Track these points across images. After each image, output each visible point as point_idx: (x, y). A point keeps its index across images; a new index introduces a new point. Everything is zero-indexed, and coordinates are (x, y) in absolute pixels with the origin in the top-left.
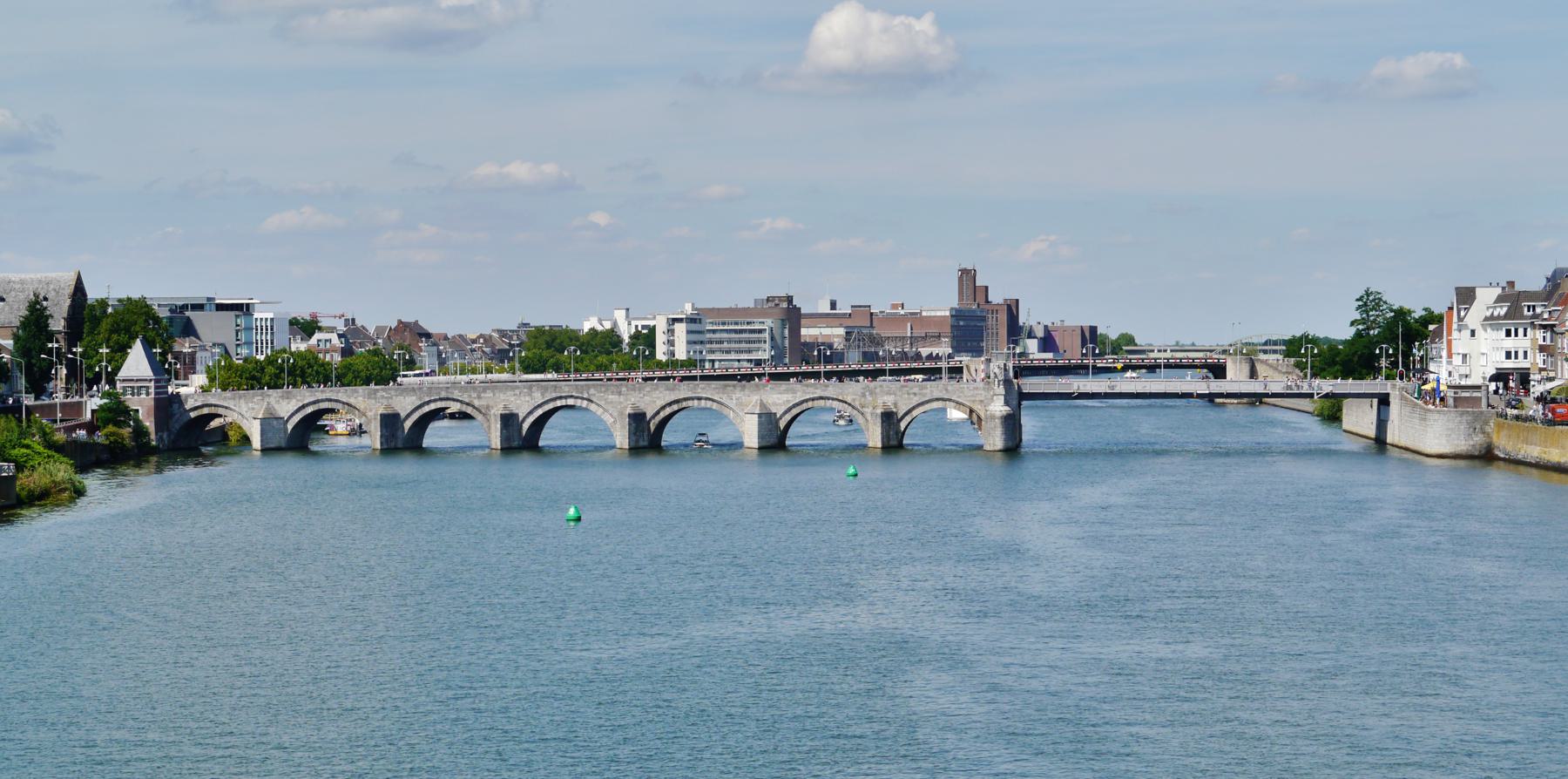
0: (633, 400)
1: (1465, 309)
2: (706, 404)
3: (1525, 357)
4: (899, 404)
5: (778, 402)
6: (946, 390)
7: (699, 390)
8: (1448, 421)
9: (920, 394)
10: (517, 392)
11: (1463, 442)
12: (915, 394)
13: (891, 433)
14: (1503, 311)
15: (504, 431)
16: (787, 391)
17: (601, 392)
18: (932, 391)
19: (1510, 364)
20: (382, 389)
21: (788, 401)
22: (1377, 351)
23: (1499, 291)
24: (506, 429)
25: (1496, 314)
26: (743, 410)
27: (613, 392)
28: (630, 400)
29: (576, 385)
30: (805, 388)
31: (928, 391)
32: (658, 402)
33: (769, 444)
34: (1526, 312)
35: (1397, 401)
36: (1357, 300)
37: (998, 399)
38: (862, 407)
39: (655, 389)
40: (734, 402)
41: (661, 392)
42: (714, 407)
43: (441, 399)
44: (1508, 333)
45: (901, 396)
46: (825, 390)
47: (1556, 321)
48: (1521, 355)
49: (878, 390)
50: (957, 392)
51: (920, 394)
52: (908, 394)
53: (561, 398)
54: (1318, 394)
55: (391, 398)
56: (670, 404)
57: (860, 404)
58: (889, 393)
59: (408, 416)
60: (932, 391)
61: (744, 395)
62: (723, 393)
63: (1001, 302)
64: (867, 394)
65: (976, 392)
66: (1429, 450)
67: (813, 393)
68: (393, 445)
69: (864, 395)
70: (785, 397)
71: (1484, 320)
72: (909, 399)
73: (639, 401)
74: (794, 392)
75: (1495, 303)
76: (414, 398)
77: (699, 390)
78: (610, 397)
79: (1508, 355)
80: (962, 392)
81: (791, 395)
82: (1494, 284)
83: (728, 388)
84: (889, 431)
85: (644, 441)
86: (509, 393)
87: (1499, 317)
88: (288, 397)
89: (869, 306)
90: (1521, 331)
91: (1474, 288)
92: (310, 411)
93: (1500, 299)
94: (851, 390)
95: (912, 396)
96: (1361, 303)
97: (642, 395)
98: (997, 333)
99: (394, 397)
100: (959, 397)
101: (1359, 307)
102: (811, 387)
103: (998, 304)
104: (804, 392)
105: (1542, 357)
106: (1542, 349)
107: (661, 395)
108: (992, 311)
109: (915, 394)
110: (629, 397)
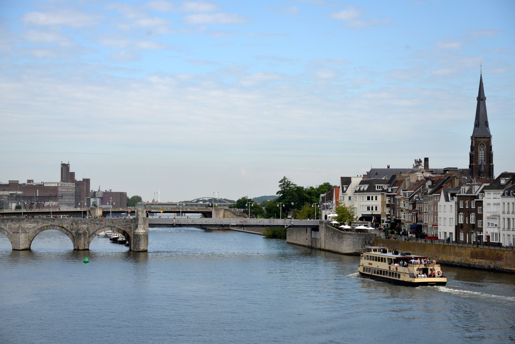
1: (346, 187)
3: (376, 210)
4: (90, 229)
5: (30, 227)
6: (113, 222)
8: (354, 238)
9: (100, 224)
11: (361, 248)
12: (97, 224)
13: (86, 243)
14: (366, 188)
16: (34, 222)
18: (105, 223)
19: (369, 213)
21: (35, 227)
22: (278, 206)
23: (361, 179)
25: (362, 189)
26: (12, 231)
30: (44, 221)
31: (104, 223)
33: (24, 248)
34: (376, 189)
35: (323, 229)
36: (279, 182)
37: (140, 226)
38: (71, 230)
40: (8, 227)
44: (368, 198)
46: (52, 222)
47: (395, 193)
48: (374, 208)
49: (79, 222)
50: (118, 223)
51: (100, 224)
52: (94, 224)
54: (286, 226)
57: (71, 229)
58: (85, 224)
60: (105, 223)
61: (13, 224)
62: (2, 223)
63: (81, 180)
64: (74, 224)
66: (344, 252)
67: (49, 223)
69: (72, 224)
70: (33, 225)
71: (355, 192)
72: (95, 227)
74: (38, 222)
75: (359, 185)
79: (368, 209)
80: (120, 223)
81: (36, 224)
82: (359, 176)
83: (4, 220)
84: (85, 242)
87: (363, 191)
89: (18, 181)
90: (374, 198)
91: (351, 177)
93: (362, 183)
94: (66, 222)
95: (96, 225)
96: (281, 183)
98: (80, 195)
100: (118, 226)
101: (280, 186)
102: (46, 220)
103: (80, 181)
104: (43, 223)
105: (388, 210)
106: (388, 206)
108: (78, 184)
109: (97, 224)
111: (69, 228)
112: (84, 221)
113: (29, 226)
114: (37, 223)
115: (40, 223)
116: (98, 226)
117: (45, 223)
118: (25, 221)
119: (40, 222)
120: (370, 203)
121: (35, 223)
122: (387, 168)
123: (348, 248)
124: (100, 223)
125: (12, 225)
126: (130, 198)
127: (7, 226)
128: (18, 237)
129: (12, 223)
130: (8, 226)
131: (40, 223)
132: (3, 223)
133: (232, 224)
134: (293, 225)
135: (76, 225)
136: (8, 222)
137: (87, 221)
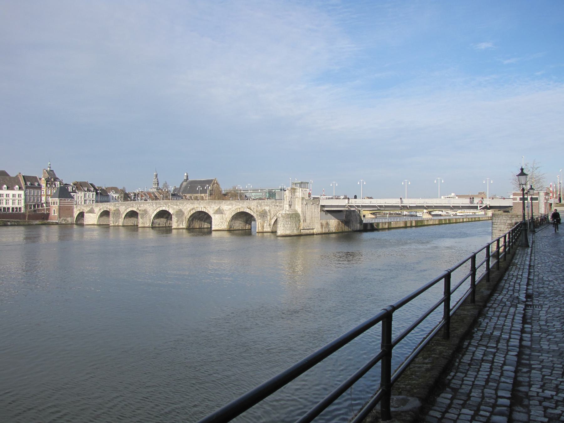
0: (181, 208)
4: (272, 210)
7: (201, 204)
9: (279, 206)
13: (265, 225)
15: (141, 220)
17: (172, 205)
20: (117, 203)
21: (230, 209)
24: (142, 219)
27: (175, 204)
29: (165, 202)
32: (188, 209)
33: (221, 228)
39: (188, 204)
45: (271, 207)
46: (243, 204)
49: (263, 204)
52: (275, 206)
53: (161, 207)
54: (480, 206)
56: (193, 209)
57: (256, 211)
58: (267, 206)
59: (123, 213)
61: (215, 206)
62: (208, 205)
64: (259, 206)
67: (239, 205)
68: (117, 224)
70: (230, 207)
73: (183, 209)
77: (201, 204)
78: (174, 206)
85: (183, 225)
86: (148, 205)
88: (97, 206)
92: (102, 211)
97: (183, 206)
104: (236, 205)
110: (180, 206)
111: (255, 210)
112: (267, 203)
113: (226, 208)
115: (234, 205)
116: (278, 208)
119: (233, 204)
121: (230, 205)
124: (280, 204)
127: (211, 208)
128: (285, 219)
130: (212, 207)
131: (234, 205)
133: (410, 205)
134: (489, 206)
135: (260, 207)
136: (213, 204)
137: (269, 203)
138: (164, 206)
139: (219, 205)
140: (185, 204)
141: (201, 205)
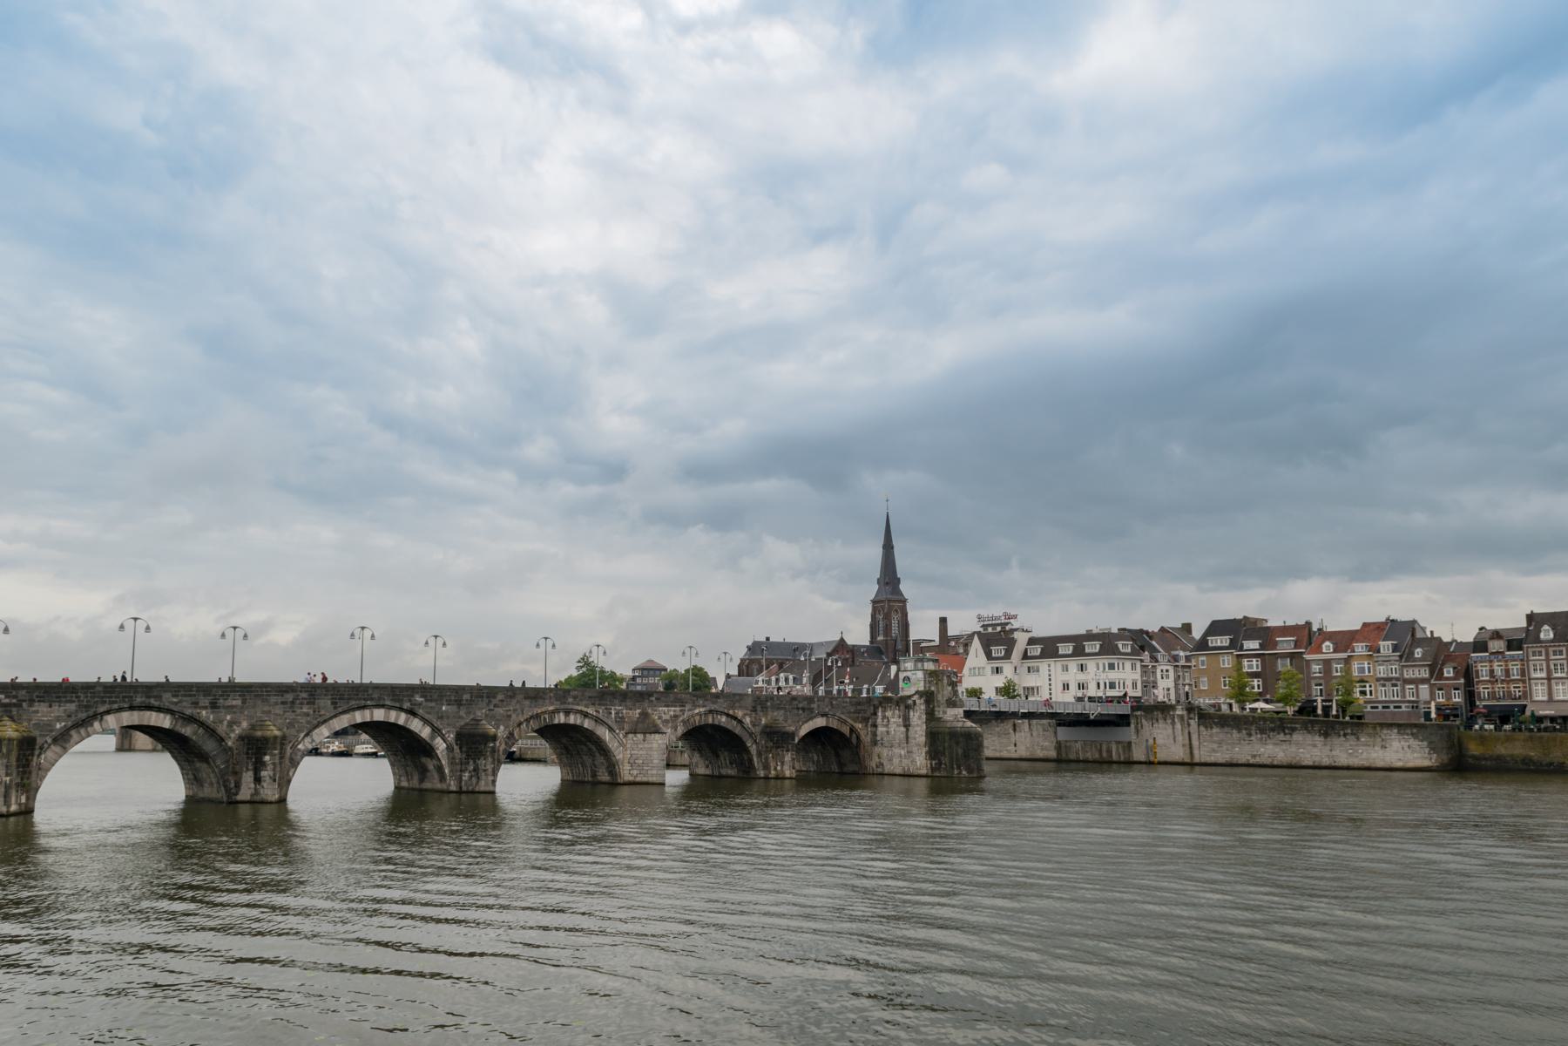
2: (576, 719)
7: (570, 700)
8: (1431, 734)
10: (290, 697)
17: (431, 701)
18: (819, 706)
28: (475, 714)
30: (695, 698)
32: (514, 716)
41: (518, 702)
42: (586, 726)
43: (132, 708)
52: (798, 709)
55: (18, 705)
62: (599, 705)
64: (759, 708)
65: (859, 707)
72: (798, 715)
74: (682, 704)
76: (72, 707)
77: (570, 700)
81: (678, 709)
86: (273, 699)
95: (801, 712)
99: (24, 704)
107: (518, 706)
109: (803, 709)
114: (680, 706)
117: (699, 706)
118: (653, 699)
119: (686, 703)
120: (1113, 676)
122: (765, 640)
123: (1415, 755)
125: (624, 711)
126: (868, 644)
127: (611, 713)
129: (624, 703)
130: (613, 712)
132: (604, 705)
138: (383, 706)
139: (637, 704)
140: (502, 701)
141: (569, 704)
